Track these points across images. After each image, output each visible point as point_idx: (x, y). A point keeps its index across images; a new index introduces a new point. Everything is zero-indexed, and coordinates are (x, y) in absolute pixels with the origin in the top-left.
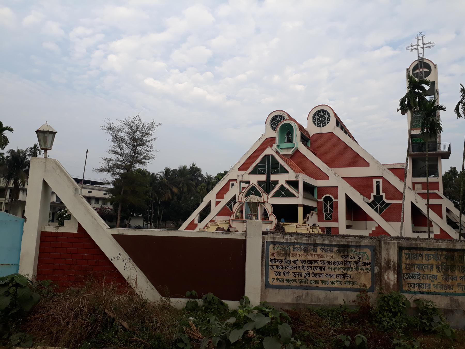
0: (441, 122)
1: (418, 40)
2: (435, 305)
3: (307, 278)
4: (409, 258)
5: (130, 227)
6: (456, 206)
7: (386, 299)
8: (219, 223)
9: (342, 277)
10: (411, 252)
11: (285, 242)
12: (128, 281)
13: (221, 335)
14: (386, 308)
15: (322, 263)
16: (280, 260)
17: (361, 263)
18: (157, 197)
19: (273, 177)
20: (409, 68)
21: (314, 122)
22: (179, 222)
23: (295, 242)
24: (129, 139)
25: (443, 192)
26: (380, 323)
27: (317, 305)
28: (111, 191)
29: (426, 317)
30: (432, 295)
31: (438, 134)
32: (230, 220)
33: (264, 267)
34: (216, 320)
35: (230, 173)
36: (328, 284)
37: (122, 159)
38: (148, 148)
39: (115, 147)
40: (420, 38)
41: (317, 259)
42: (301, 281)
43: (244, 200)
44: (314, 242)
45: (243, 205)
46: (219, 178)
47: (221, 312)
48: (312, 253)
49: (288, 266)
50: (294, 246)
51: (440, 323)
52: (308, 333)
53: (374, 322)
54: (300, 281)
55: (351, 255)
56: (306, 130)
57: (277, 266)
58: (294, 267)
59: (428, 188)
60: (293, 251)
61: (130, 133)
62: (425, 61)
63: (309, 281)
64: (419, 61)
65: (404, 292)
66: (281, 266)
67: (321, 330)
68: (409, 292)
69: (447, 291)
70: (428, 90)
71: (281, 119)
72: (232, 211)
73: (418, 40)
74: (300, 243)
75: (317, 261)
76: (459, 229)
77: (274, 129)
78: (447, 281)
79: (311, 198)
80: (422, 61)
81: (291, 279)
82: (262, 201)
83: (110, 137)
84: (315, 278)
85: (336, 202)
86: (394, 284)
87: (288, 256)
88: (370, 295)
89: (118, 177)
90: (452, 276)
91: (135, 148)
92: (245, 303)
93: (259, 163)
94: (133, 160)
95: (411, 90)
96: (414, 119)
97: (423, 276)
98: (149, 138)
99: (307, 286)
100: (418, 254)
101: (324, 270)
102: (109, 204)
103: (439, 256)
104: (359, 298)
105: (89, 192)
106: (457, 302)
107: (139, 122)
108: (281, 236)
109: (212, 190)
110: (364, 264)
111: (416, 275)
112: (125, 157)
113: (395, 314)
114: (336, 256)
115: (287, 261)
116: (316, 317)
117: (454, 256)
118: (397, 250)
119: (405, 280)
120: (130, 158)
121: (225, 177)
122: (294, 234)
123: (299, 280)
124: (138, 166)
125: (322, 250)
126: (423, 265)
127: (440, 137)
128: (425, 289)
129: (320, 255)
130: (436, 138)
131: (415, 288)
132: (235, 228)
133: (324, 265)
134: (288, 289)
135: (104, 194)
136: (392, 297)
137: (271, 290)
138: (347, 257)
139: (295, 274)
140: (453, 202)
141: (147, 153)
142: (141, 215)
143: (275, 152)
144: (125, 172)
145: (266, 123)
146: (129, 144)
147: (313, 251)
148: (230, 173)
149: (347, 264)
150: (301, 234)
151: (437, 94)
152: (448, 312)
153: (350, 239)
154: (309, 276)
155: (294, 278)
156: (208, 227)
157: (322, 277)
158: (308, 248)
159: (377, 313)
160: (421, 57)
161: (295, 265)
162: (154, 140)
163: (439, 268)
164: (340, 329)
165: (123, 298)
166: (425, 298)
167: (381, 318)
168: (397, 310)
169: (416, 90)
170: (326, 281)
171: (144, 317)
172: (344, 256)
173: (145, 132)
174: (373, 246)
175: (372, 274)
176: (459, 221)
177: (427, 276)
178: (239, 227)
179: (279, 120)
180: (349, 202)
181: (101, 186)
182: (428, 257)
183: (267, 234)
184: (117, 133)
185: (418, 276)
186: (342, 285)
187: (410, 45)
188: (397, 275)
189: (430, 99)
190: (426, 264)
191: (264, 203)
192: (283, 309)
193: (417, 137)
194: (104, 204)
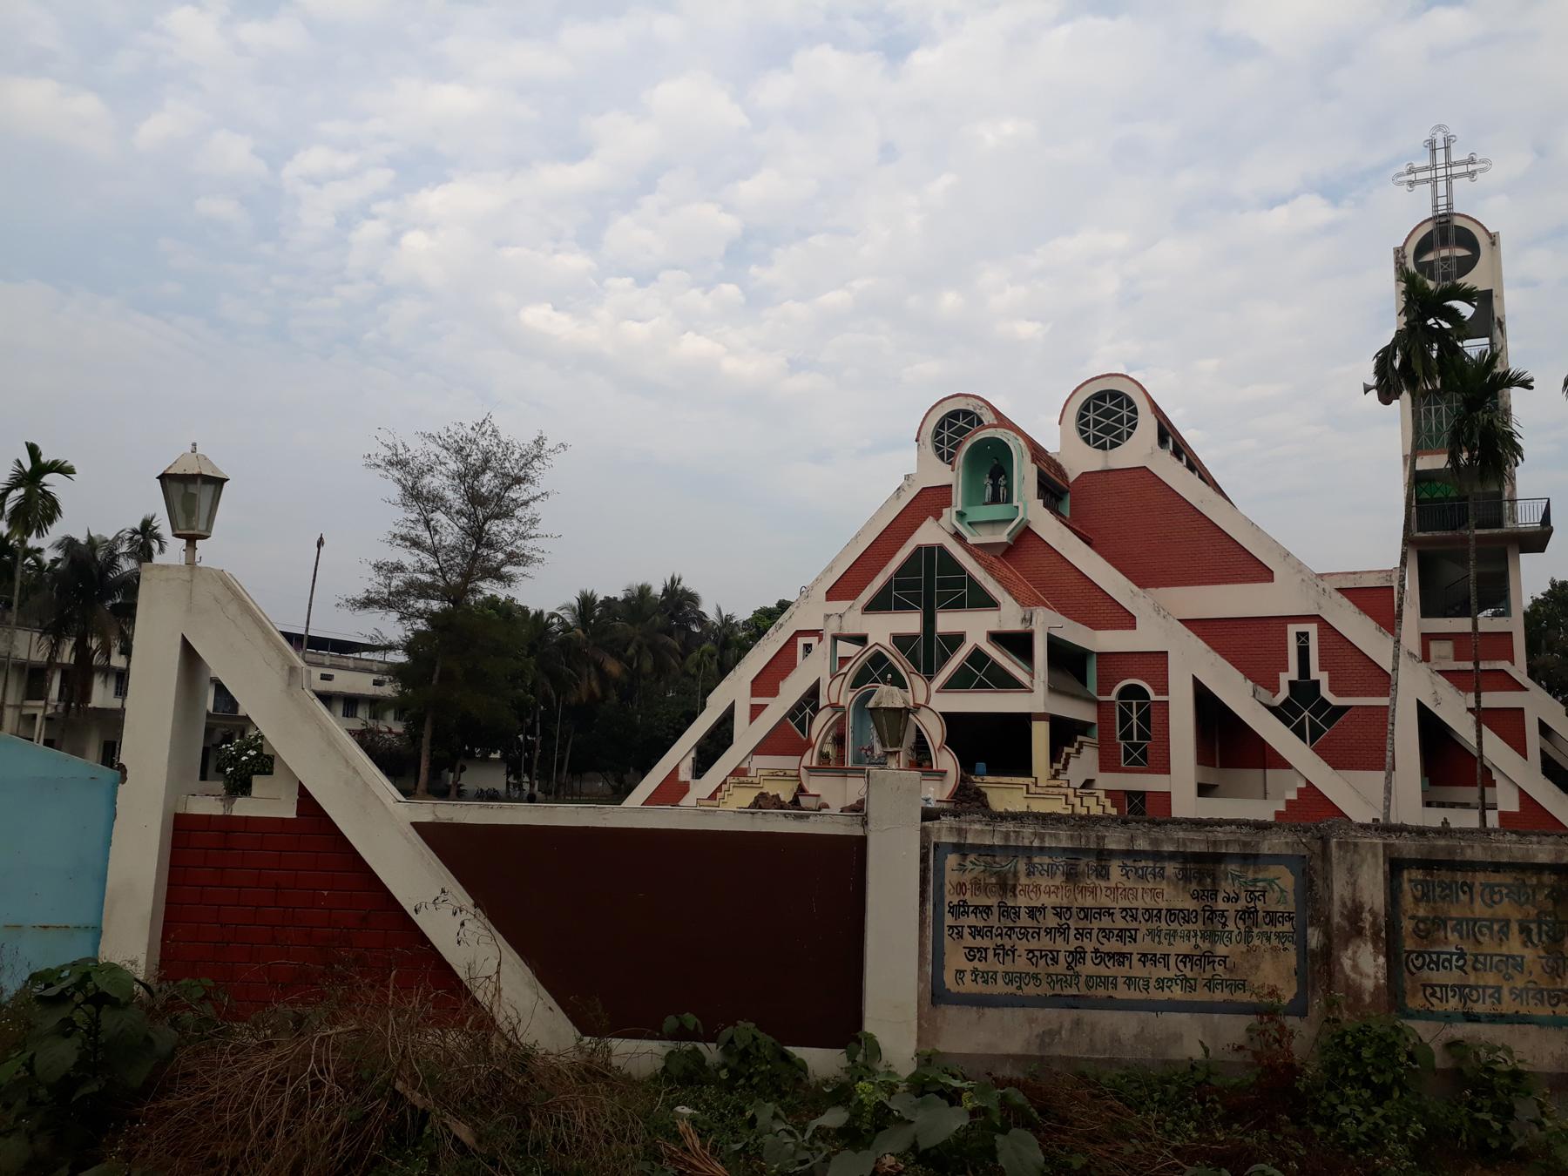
1: (1434, 150)
2: (1519, 1061)
4: (1425, 896)
5: (461, 795)
8: (762, 778)
9: (1197, 965)
10: (1432, 877)
11: (1000, 846)
14: (1352, 1072)
15: (1128, 918)
16: (983, 906)
17: (1261, 914)
19: (946, 622)
21: (1082, 432)
22: (625, 776)
23: (1034, 844)
24: (459, 496)
27: (1111, 1062)
28: (397, 671)
29: (1488, 1103)
30: (1508, 1026)
32: (799, 770)
33: (930, 932)
35: (797, 607)
36: (1146, 990)
37: (437, 566)
38: (523, 528)
39: (412, 525)
40: (1440, 144)
41: (1108, 903)
42: (1054, 978)
45: (844, 715)
48: (1094, 883)
49: (1011, 929)
50: (1029, 858)
51: (1540, 1125)
52: (1084, 1161)
53: (1308, 1120)
54: (1053, 979)
55: (1227, 887)
56: (1054, 461)
57: (974, 927)
60: (1028, 875)
61: (461, 477)
62: (1458, 222)
63: (1082, 979)
64: (1437, 221)
65: (1410, 1016)
66: (985, 929)
67: (1128, 1149)
68: (1429, 1015)
69: (1557, 1010)
70: (1470, 319)
71: (971, 423)
73: (1434, 150)
74: (1050, 848)
75: (1111, 911)
77: (947, 457)
78: (1559, 976)
81: (1021, 973)
83: (396, 492)
84: (1102, 971)
85: (1162, 704)
86: (1377, 987)
88: (1291, 1026)
89: (421, 625)
92: (866, 1056)
93: (898, 573)
94: (471, 568)
95: (1415, 320)
96: (1425, 419)
97: (1476, 960)
98: (526, 493)
99: (1075, 996)
100: (1457, 883)
101: (1135, 942)
102: (390, 715)
104: (1254, 1035)
105: (325, 677)
107: (491, 440)
110: (1271, 921)
111: (1451, 957)
112: (445, 558)
113: (1381, 1094)
114: (1174, 893)
115: (1007, 911)
116: (1110, 1103)
118: (1384, 872)
119: (1413, 974)
121: (780, 621)
123: (1049, 975)
124: (489, 588)
127: (1514, 478)
128: (1484, 1003)
129: (1120, 891)
130: (1501, 486)
131: (1447, 1001)
132: (818, 796)
133: (1134, 925)
134: (1013, 1006)
135: (374, 684)
136: (1370, 1032)
137: (952, 1011)
138: (1213, 896)
139: (1034, 956)
141: (519, 543)
142: (499, 752)
143: (952, 536)
144: (445, 610)
145: (920, 439)
146: (460, 512)
147: (1097, 877)
148: (797, 607)
151: (1502, 332)
154: (1081, 960)
155: (1032, 970)
156: (727, 793)
157: (1127, 963)
159: (1319, 1089)
160: (1445, 207)
161: (1035, 924)
162: (541, 498)
163: (1531, 930)
164: (1193, 1147)
166: (1482, 1037)
167: (1334, 1107)
168: (1389, 1077)
169: (1431, 321)
172: (1203, 891)
175: (1298, 955)
177: (1489, 958)
178: (836, 792)
179: (961, 426)
181: (365, 655)
182: (1492, 893)
184: (418, 477)
185: (1457, 961)
186: (1195, 990)
189: (1477, 353)
190: (1486, 916)
191: (917, 707)
192: (994, 1075)
194: (374, 718)
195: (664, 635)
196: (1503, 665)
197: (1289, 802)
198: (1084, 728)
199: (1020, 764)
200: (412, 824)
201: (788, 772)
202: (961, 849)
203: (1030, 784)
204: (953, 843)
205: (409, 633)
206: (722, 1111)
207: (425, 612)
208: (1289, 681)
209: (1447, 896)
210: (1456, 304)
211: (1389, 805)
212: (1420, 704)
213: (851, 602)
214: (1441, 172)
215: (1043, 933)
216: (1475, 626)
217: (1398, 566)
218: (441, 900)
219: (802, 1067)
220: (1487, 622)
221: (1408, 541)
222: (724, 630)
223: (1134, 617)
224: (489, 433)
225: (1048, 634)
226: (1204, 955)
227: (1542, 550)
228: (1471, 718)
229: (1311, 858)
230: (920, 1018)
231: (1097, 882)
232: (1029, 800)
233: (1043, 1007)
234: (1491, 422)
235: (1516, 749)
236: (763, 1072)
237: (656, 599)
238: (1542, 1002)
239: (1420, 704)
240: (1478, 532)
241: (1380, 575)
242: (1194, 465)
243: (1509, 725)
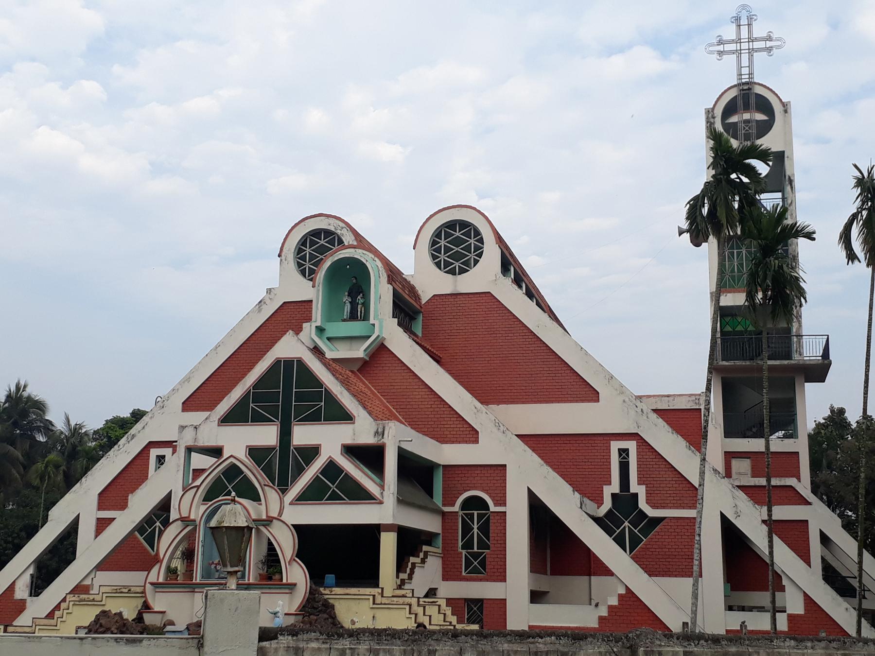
0: (801, 273)
6: (848, 526)
8: (105, 595)
20: (712, 107)
21: (434, 257)
25: (812, 483)
31: (795, 311)
32: (144, 586)
35: (151, 418)
43: (198, 512)
45: (195, 529)
46: (112, 435)
56: (408, 283)
59: (768, 475)
62: (758, 90)
64: (741, 88)
71: (332, 243)
72: (153, 553)
76: (856, 598)
77: (308, 274)
80: (749, 89)
82: (260, 514)
93: (257, 385)
95: (720, 174)
96: (728, 261)
108: (323, 643)
109: (83, 479)
122: (367, 634)
127: (801, 317)
130: (790, 321)
132: (164, 612)
140: (839, 516)
145: (283, 254)
150: (389, 635)
151: (792, 188)
156: (65, 611)
169: (734, 176)
176: (857, 574)
179: (322, 244)
183: (276, 638)
187: (715, 41)
189: (772, 205)
191: (268, 521)
193: (736, 315)
195: (5, 444)
196: (791, 482)
197: (611, 608)
198: (428, 538)
201: (133, 589)
203: (377, 595)
208: (612, 494)
210: (754, 162)
211: (696, 610)
212: (723, 516)
213: (207, 414)
214: (745, 46)
217: (705, 391)
220: (778, 443)
221: (713, 368)
222: (72, 440)
223: (477, 432)
225: (399, 447)
227: (823, 380)
228: (765, 528)
232: (375, 610)
234: (781, 267)
239: (723, 516)
240: (770, 362)
241: (691, 399)
242: (532, 293)
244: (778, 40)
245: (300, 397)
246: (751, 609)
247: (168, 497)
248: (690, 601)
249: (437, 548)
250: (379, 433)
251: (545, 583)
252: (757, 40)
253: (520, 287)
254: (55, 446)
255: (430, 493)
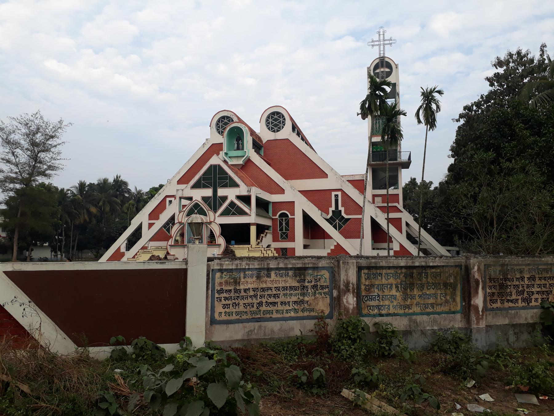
0: (401, 128)
1: (380, 35)
3: (260, 309)
4: (368, 278)
5: (32, 260)
6: (416, 220)
7: (345, 325)
11: (235, 269)
12: (29, 331)
13: (155, 387)
14: (345, 335)
15: (277, 290)
17: (319, 286)
18: (69, 220)
19: (221, 192)
20: (369, 66)
21: (267, 126)
22: (100, 251)
23: (246, 267)
25: (403, 205)
26: (339, 352)
27: (271, 339)
29: (385, 341)
31: (399, 142)
33: (210, 300)
34: (148, 369)
38: (55, 156)
40: (381, 33)
41: (270, 286)
42: (252, 312)
43: (185, 220)
44: (267, 266)
45: (184, 226)
47: (157, 359)
49: (238, 297)
50: (245, 272)
51: (399, 346)
52: (261, 373)
54: (252, 313)
55: (308, 278)
56: (258, 136)
58: (245, 297)
61: (28, 135)
62: (387, 60)
63: (262, 312)
65: (363, 316)
67: (275, 367)
68: (368, 315)
69: (405, 311)
70: (389, 92)
72: (169, 235)
73: (380, 35)
74: (252, 268)
76: (417, 244)
77: (221, 133)
79: (264, 215)
80: (383, 59)
81: (241, 312)
82: (207, 220)
84: (268, 308)
86: (354, 308)
87: (238, 285)
89: (12, 194)
90: (411, 295)
91: (36, 155)
92: (187, 345)
93: (204, 174)
94: (33, 171)
97: (383, 297)
99: (260, 318)
100: (378, 273)
103: (399, 275)
104: (316, 326)
106: (415, 322)
107: (40, 121)
109: (143, 209)
110: (322, 288)
112: (21, 167)
113: (354, 341)
114: (292, 281)
116: (270, 353)
117: (413, 273)
118: (356, 271)
120: (28, 169)
121: (160, 192)
123: (251, 311)
124: (41, 179)
125: (277, 275)
126: (383, 285)
129: (274, 281)
130: (397, 146)
133: (279, 292)
137: (217, 327)
140: (413, 216)
141: (53, 161)
144: (22, 188)
146: (27, 149)
149: (303, 289)
152: (407, 333)
153: (306, 261)
155: (245, 310)
157: (276, 305)
158: (260, 274)
159: (336, 342)
161: (246, 294)
164: (296, 364)
165: (21, 353)
167: (340, 347)
169: (377, 92)
170: (280, 310)
171: (52, 376)
172: (301, 280)
173: (49, 134)
174: (331, 267)
176: (418, 236)
178: (179, 253)
180: (307, 220)
187: (371, 41)
188: (357, 298)
191: (210, 223)
192: (232, 347)
197: (332, 250)
198: (268, 227)
199: (246, 240)
200: (3, 272)
201: (163, 247)
202: (221, 271)
204: (218, 269)
205: (7, 197)
206: (132, 369)
207: (13, 189)
209: (375, 277)
210: (386, 87)
212: (371, 217)
214: (382, 43)
215: (249, 297)
216: (388, 192)
217: (365, 173)
218: (14, 301)
219: (164, 351)
221: (368, 165)
222: (138, 196)
224: (39, 118)
226: (301, 301)
228: (386, 221)
229: (334, 267)
230: (206, 330)
231: (267, 279)
233: (248, 322)
234: (394, 126)
235: (400, 232)
236: (148, 354)
237: (111, 184)
238: (401, 309)
239: (371, 217)
242: (303, 139)
243: (397, 223)
244: (394, 40)
245: (220, 178)
246: (381, 249)
247: (174, 216)
248: (359, 246)
249: (270, 231)
250: (249, 191)
251: (308, 242)
252: (386, 40)
253: (299, 136)
254: (132, 198)
255: (268, 212)
